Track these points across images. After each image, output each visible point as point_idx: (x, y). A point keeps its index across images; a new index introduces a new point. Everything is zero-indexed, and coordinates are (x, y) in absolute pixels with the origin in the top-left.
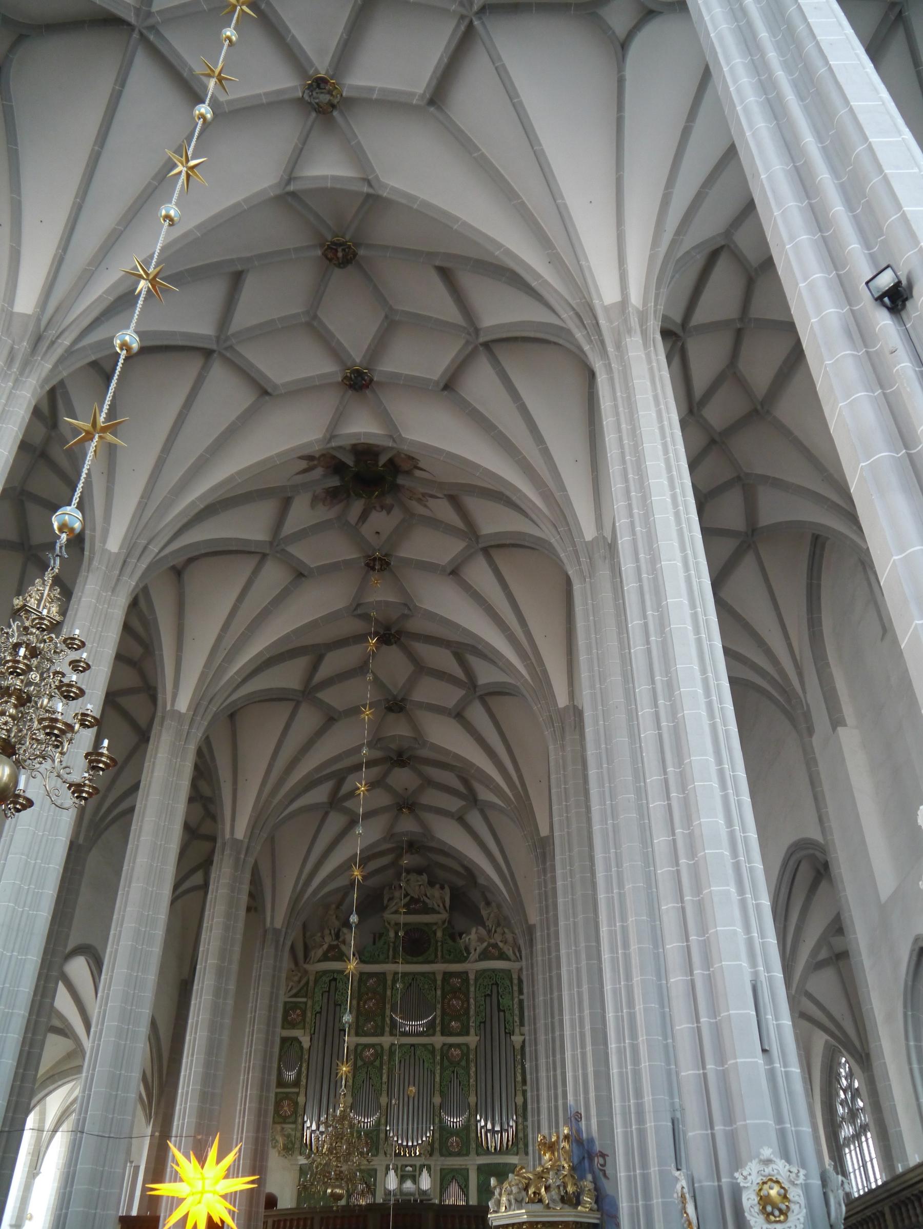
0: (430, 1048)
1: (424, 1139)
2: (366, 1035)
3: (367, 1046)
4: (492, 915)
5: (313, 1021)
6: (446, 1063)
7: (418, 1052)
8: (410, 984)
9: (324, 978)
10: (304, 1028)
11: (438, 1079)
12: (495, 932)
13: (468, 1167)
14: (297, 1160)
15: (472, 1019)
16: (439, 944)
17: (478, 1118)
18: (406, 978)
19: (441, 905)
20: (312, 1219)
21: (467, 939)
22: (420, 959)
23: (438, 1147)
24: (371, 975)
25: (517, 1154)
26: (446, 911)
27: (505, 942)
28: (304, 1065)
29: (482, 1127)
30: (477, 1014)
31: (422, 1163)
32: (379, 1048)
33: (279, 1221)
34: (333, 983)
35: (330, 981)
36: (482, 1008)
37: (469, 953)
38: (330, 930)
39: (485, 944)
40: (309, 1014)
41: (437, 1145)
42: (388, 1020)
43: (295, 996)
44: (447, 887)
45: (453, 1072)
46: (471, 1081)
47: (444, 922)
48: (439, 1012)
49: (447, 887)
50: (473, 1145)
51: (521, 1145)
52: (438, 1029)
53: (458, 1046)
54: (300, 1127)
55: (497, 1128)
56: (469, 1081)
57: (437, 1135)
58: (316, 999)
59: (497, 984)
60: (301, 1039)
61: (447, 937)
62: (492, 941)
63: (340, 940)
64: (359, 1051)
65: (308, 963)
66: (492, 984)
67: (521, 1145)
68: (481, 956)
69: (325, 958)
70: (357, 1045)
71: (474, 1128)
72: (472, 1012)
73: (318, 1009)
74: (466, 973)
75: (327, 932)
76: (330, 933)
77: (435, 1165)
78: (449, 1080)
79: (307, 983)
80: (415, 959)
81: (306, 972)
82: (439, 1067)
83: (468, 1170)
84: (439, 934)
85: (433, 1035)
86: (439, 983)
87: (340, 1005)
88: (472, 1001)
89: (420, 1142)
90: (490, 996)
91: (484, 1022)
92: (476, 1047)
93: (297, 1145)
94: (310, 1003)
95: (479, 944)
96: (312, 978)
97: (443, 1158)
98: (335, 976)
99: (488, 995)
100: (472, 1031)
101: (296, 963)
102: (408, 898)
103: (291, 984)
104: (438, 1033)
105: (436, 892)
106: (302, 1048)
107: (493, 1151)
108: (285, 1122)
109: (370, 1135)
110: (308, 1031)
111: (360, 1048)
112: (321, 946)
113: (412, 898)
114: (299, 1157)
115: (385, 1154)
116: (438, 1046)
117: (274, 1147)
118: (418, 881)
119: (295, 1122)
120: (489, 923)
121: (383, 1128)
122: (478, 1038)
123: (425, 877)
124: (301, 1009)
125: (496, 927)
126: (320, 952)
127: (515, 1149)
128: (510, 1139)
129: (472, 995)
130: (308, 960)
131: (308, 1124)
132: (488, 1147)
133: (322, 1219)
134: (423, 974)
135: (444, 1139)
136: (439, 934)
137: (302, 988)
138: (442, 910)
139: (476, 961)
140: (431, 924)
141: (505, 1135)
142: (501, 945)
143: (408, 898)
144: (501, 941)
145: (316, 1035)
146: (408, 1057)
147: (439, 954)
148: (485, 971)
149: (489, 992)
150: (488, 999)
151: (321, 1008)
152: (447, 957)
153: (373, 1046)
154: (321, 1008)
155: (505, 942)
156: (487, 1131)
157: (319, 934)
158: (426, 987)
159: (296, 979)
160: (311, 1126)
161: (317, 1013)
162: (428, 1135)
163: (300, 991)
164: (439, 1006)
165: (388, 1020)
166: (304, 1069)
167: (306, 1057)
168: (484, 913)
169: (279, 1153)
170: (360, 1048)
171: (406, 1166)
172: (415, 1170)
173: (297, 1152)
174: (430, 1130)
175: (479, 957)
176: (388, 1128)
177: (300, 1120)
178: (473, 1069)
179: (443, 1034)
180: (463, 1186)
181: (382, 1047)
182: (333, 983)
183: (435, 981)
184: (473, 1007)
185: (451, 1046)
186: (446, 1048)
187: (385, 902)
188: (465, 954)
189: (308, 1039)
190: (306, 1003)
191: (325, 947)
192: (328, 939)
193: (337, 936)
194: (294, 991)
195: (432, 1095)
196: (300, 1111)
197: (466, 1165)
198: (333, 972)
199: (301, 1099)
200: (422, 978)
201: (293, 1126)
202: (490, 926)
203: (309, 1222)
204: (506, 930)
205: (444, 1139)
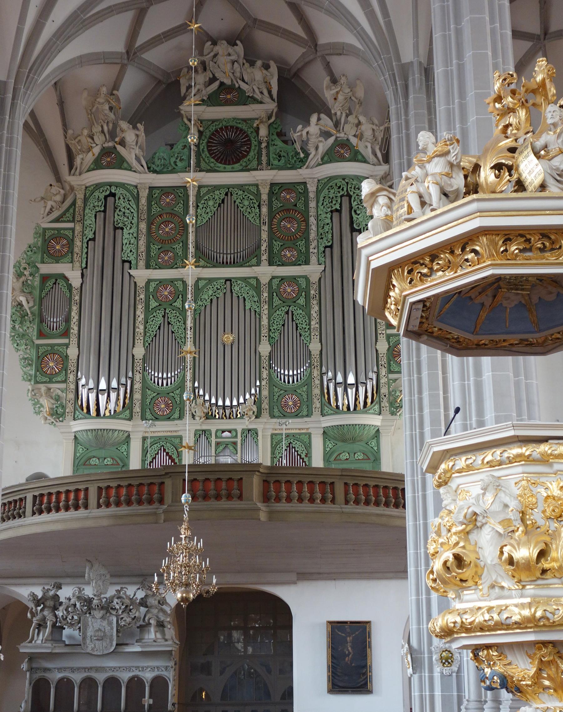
0: (254, 282)
1: (248, 396)
2: (160, 267)
3: (162, 283)
4: (341, 97)
5: (85, 251)
6: (277, 301)
7: (236, 288)
8: (223, 201)
9: (96, 194)
10: (72, 262)
11: (265, 322)
12: (346, 122)
13: (309, 431)
14: (70, 426)
15: (314, 244)
16: (264, 145)
17: (324, 369)
18: (217, 192)
19: (265, 92)
20: (87, 489)
21: (304, 133)
22: (237, 166)
23: (267, 407)
24: (166, 191)
25: (380, 414)
26: (273, 100)
27: (360, 137)
28: (75, 308)
29: (329, 380)
30: (320, 237)
31: (245, 427)
32: (179, 285)
33: (42, 495)
34: (110, 200)
35: (106, 197)
36: (327, 228)
37: (307, 155)
38: (102, 127)
39: (331, 140)
40: (78, 243)
41: (265, 405)
42: (191, 249)
43: (57, 220)
44: (272, 63)
45: (287, 313)
46: (313, 323)
47: (269, 118)
48: (265, 236)
49: (272, 63)
50: (317, 404)
51: (385, 403)
52: (264, 257)
53: (293, 279)
54: (73, 386)
55: (351, 379)
56: (310, 324)
57: (265, 393)
58: (87, 222)
59: (350, 197)
60: (68, 274)
61: (275, 137)
62: (342, 135)
63: (117, 139)
64: (151, 290)
65: (74, 175)
66: (341, 196)
67: (385, 403)
68: (326, 158)
69: (97, 165)
70: (149, 282)
71: (317, 382)
72: (313, 235)
73: (91, 236)
74: (305, 184)
75: (97, 129)
76: (103, 132)
77: (264, 429)
78: (282, 323)
79: (74, 203)
80: (229, 167)
81: (72, 189)
82: (266, 307)
83: (310, 435)
84: (263, 132)
85: (258, 264)
86: (264, 197)
87: (122, 229)
88: (312, 220)
89: (241, 400)
90: (339, 211)
91: (331, 247)
92: (320, 278)
93: (70, 408)
94: (78, 228)
95: (321, 139)
96: (80, 196)
97: (275, 420)
98: (113, 191)
99: (337, 210)
100: (313, 259)
101: (59, 179)
102: (216, 84)
103: (50, 204)
104: (265, 262)
105: (258, 74)
106: (70, 287)
107: (345, 409)
108: (50, 382)
109: (172, 394)
110: (77, 264)
111: (153, 285)
112: (90, 149)
113: (222, 84)
114: (73, 423)
115: (193, 416)
116: (264, 280)
117: (38, 413)
118: (229, 55)
119: (65, 381)
120: (337, 109)
121: (189, 384)
122: (322, 268)
123: (240, 48)
124: (65, 237)
125: (347, 116)
126: (90, 158)
127: (377, 407)
128: (369, 395)
129: (312, 212)
130: (73, 171)
131: (83, 381)
132: (337, 407)
133: (100, 489)
134: (241, 187)
135: (276, 398)
136: (263, 132)
137: (67, 210)
138: (267, 99)
139: (321, 165)
140: (250, 119)
141: (362, 390)
142: (354, 141)
143: (216, 84)
144: (355, 136)
145: (88, 272)
146: (222, 294)
147: (264, 159)
148: (331, 179)
149: (338, 207)
150: (336, 215)
151: (94, 233)
152: (276, 162)
153: (172, 281)
154: (94, 233)
155: (360, 137)
156: (336, 385)
157: (86, 132)
158: (246, 203)
159: (58, 198)
160: (87, 383)
161: (90, 239)
162: (253, 391)
163: (64, 214)
164: (265, 228)
165: (191, 249)
166: (74, 314)
167: (77, 298)
168: (328, 95)
169: (46, 419)
170: (153, 285)
171: (223, 432)
172: (236, 436)
173: (69, 417)
174: (256, 386)
175: (322, 159)
176: (196, 384)
177: (72, 377)
178: (316, 308)
179: (271, 264)
180: (303, 456)
181: (184, 283)
182: (110, 200)
183: (258, 195)
184: (314, 228)
185: (282, 279)
186: (276, 282)
187: (183, 90)
188: (302, 155)
189: (79, 273)
190: (73, 230)
191: (97, 150)
192: (99, 139)
193: (113, 134)
194: (56, 214)
195: (258, 341)
196: (72, 367)
197: (308, 429)
198: (110, 185)
199: (72, 352)
200: (240, 192)
201: (63, 386)
202: (339, 113)
203: (82, 495)
204: (362, 119)
205: (276, 398)
